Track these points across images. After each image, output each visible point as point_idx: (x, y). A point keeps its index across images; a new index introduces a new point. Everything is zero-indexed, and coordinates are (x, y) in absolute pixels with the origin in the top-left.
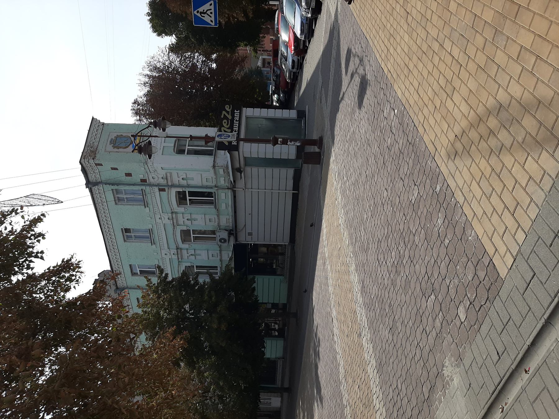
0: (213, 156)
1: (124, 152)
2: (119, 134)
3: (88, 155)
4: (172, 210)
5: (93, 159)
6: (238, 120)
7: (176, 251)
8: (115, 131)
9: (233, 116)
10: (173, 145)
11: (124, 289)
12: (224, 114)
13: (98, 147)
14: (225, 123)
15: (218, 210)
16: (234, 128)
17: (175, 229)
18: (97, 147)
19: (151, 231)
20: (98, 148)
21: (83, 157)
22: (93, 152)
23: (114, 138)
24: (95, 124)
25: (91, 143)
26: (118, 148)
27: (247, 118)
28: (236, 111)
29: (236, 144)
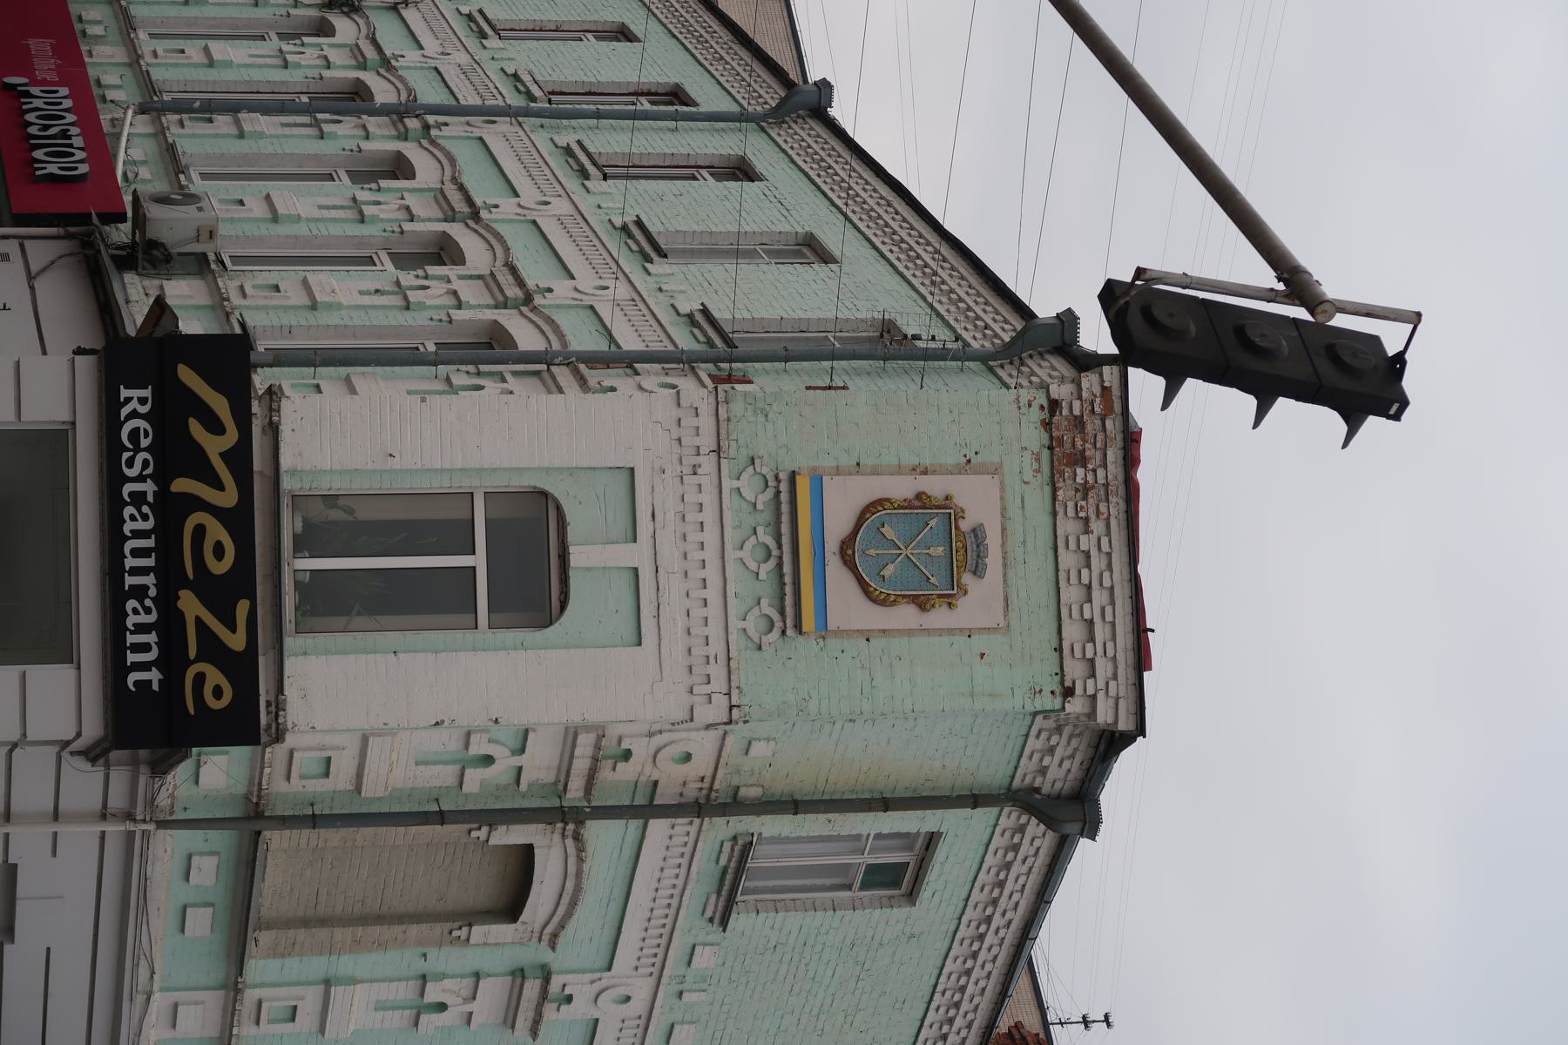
0: (287, 484)
1: (876, 472)
2: (939, 617)
3: (1092, 425)
4: (534, 309)
5: (1054, 405)
6: (132, 604)
7: (484, 214)
8: (979, 643)
9: (170, 624)
10: (579, 557)
11: (778, 115)
14: (219, 551)
15: (228, 315)
17: (499, 263)
18: (1054, 498)
19: (653, 255)
20: (1048, 489)
21: (1117, 407)
23: (967, 579)
24: (1115, 677)
25: (1097, 526)
27: (62, 651)
28: (154, 676)
29: (125, 393)
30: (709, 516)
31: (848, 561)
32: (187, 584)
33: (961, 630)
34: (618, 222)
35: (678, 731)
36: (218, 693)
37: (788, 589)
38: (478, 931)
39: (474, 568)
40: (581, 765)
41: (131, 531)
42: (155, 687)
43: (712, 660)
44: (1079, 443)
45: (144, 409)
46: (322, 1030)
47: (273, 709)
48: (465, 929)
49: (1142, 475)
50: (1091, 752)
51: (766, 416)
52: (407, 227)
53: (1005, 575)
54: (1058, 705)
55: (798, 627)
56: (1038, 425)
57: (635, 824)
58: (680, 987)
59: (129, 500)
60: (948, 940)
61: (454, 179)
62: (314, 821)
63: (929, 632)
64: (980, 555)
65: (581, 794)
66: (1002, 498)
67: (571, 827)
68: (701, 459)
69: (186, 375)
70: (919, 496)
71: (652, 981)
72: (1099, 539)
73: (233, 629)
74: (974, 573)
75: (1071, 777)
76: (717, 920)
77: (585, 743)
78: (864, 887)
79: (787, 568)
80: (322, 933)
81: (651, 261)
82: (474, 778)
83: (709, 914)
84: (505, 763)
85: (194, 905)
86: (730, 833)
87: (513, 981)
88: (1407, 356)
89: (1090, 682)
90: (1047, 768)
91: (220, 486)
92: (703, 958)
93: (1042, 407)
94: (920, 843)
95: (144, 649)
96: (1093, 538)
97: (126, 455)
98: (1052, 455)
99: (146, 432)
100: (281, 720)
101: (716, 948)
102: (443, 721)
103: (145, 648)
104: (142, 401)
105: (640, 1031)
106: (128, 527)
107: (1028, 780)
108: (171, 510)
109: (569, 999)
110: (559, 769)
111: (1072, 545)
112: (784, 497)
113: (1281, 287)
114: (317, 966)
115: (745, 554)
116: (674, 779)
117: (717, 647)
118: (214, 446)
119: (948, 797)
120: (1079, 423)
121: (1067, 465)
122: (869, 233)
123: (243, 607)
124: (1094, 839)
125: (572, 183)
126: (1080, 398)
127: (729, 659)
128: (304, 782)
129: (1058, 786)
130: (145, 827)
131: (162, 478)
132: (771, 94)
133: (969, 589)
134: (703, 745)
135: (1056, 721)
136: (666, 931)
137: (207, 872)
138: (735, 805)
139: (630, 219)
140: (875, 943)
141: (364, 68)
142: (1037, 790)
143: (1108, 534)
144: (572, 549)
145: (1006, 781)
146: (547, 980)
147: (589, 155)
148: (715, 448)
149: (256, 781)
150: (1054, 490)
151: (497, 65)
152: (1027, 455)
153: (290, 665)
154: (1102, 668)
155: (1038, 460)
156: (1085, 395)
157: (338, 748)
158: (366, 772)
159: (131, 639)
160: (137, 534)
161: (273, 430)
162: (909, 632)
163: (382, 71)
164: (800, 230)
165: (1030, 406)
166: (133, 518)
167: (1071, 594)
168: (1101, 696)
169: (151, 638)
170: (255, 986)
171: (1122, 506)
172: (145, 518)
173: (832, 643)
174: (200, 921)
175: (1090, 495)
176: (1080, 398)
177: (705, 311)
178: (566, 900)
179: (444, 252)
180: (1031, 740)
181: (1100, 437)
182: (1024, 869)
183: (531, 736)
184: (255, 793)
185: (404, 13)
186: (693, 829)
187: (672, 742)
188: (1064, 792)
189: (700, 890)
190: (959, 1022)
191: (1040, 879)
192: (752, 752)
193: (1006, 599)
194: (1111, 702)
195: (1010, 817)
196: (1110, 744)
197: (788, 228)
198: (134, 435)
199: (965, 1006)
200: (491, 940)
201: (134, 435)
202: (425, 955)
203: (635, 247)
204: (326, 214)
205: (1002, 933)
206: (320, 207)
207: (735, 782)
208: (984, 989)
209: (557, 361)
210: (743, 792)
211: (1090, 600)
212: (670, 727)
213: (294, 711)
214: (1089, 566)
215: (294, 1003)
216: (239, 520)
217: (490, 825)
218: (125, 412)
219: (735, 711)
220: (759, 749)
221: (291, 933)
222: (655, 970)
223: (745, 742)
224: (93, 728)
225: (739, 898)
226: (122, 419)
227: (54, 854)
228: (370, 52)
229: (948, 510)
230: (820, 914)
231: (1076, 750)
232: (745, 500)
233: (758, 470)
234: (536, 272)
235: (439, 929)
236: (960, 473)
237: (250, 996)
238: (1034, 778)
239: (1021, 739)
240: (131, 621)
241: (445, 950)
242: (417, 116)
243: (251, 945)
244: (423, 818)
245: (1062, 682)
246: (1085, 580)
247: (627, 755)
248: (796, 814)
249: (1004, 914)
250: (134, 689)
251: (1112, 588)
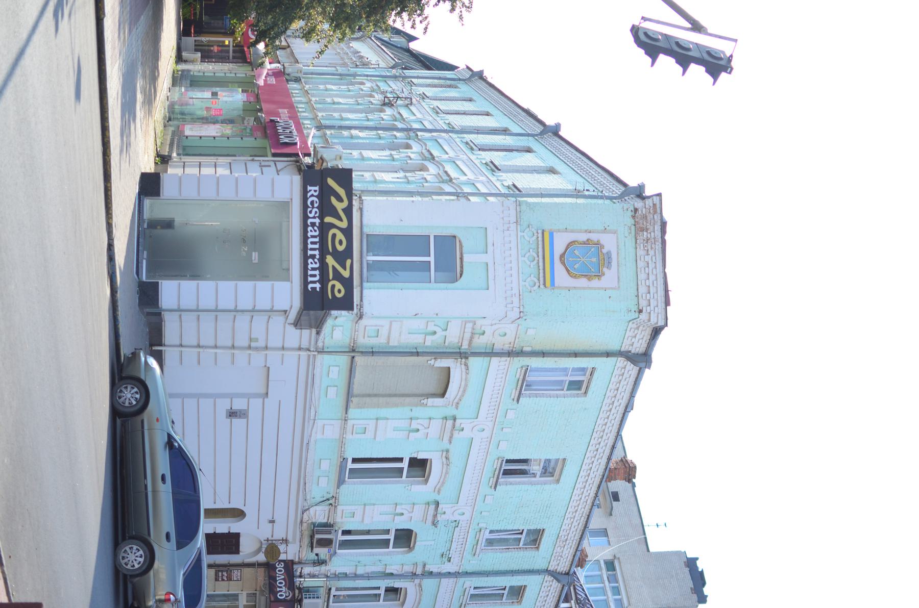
0: (366, 230)
1: (572, 231)
2: (595, 283)
3: (650, 217)
6: (310, 260)
8: (609, 292)
9: (323, 267)
12: (345, 268)
13: (634, 246)
14: (341, 242)
16: (317, 233)
18: (636, 243)
21: (658, 211)
22: (642, 230)
23: (605, 270)
25: (651, 252)
26: (588, 242)
27: (288, 278)
28: (318, 286)
29: (309, 188)
30: (513, 244)
31: (563, 263)
32: (329, 253)
33: (602, 288)
34: (484, 162)
35: (502, 324)
36: (339, 291)
37: (541, 271)
38: (430, 401)
39: (430, 262)
40: (467, 336)
41: (311, 236)
42: (318, 290)
43: (514, 296)
44: (645, 223)
45: (316, 194)
46: (375, 438)
47: (359, 307)
48: (426, 400)
49: (667, 237)
50: (649, 337)
51: (534, 211)
52: (409, 161)
53: (618, 269)
54: (637, 316)
55: (544, 284)
56: (630, 217)
57: (487, 359)
58: (502, 426)
59: (310, 225)
60: (598, 411)
61: (426, 149)
62: (373, 353)
63: (591, 288)
64: (609, 263)
65: (467, 347)
66: (617, 242)
67: (463, 360)
68: (511, 225)
69: (330, 182)
70: (588, 240)
71: (493, 423)
72: (652, 257)
73: (345, 269)
74: (607, 268)
75: (642, 346)
76: (516, 399)
77: (469, 326)
78: (568, 389)
79: (541, 264)
80: (375, 400)
81: (495, 172)
83: (512, 397)
84: (440, 334)
85: (331, 386)
86: (520, 366)
87: (443, 421)
88: (733, 55)
89: (648, 308)
90: (633, 343)
91: (341, 220)
92: (511, 415)
93: (632, 211)
94: (588, 373)
95: (315, 276)
96: (650, 256)
97: (309, 209)
98: (635, 227)
99: (316, 202)
100: (361, 311)
101: (515, 411)
102: (418, 314)
103: (315, 276)
104: (315, 191)
105: (488, 443)
106: (309, 234)
107: (627, 347)
108: (324, 229)
109: (463, 430)
110: (459, 337)
111: (642, 259)
112: (540, 239)
113: (689, 26)
114: (372, 412)
115: (525, 259)
116: (501, 344)
117: (516, 291)
118: (340, 206)
119: (598, 353)
120: (645, 217)
121: (640, 231)
122: (573, 167)
123: (348, 262)
124: (649, 368)
125: (468, 152)
126: (645, 207)
127: (520, 295)
128: (369, 339)
129: (638, 350)
130: (314, 353)
131: (321, 218)
132: (538, 129)
133: (606, 273)
134: (511, 330)
135: (637, 324)
136: (497, 404)
137: (335, 370)
138: (521, 353)
139: (488, 161)
141: (396, 121)
142: (630, 352)
143: (655, 255)
144: (464, 255)
145: (618, 348)
146: (455, 419)
147: (474, 144)
148: (515, 221)
149: (353, 337)
150: (636, 240)
151: (443, 121)
152: (626, 227)
153: (365, 292)
154: (653, 303)
155: (630, 229)
156: (647, 207)
157: (382, 326)
159: (310, 273)
160: (313, 237)
161: (361, 209)
162: (584, 288)
163: (402, 121)
164: (548, 165)
165: (627, 210)
166: (311, 231)
167: (642, 276)
168: (652, 312)
169: (317, 272)
170: (351, 419)
171: (660, 246)
172: (315, 231)
173: (556, 291)
174: (332, 392)
175: (649, 241)
176: (645, 207)
177: (514, 185)
178: (462, 389)
179: (423, 168)
180: (628, 332)
181: (652, 221)
182: (626, 383)
183: (449, 323)
184: (352, 342)
185: (412, 108)
186: (507, 363)
187: (500, 328)
188: (639, 353)
189: (511, 390)
190: (602, 444)
191: (631, 387)
192: (528, 333)
193: (619, 278)
194: (656, 315)
195: (621, 361)
196: (656, 332)
197: (544, 165)
198: (312, 203)
199: (604, 437)
200: (435, 405)
201: (312, 203)
202: (411, 410)
203: (489, 168)
204: (381, 158)
205: (617, 408)
206: (379, 156)
207: (522, 345)
208: (611, 431)
209: (460, 195)
211: (648, 279)
212: (498, 322)
213: (366, 309)
214: (648, 267)
215: (365, 426)
216: (348, 232)
217: (435, 358)
218: (309, 194)
219: (521, 313)
220: (530, 332)
221: (364, 399)
222: (493, 419)
223: (526, 329)
224: (297, 303)
225: (523, 392)
226: (308, 197)
227: (282, 364)
228: (398, 116)
229: (598, 244)
230: (552, 398)
231: (644, 336)
232: (526, 239)
233: (531, 229)
234: (453, 174)
235: (416, 399)
236: (602, 233)
237: (350, 423)
239: (624, 332)
240: (310, 266)
241: (419, 408)
242: (414, 132)
243: (351, 405)
244: (411, 354)
245: (638, 308)
246: (647, 272)
247: (484, 333)
248: (543, 357)
249: (618, 401)
250: (310, 290)
251: (657, 274)
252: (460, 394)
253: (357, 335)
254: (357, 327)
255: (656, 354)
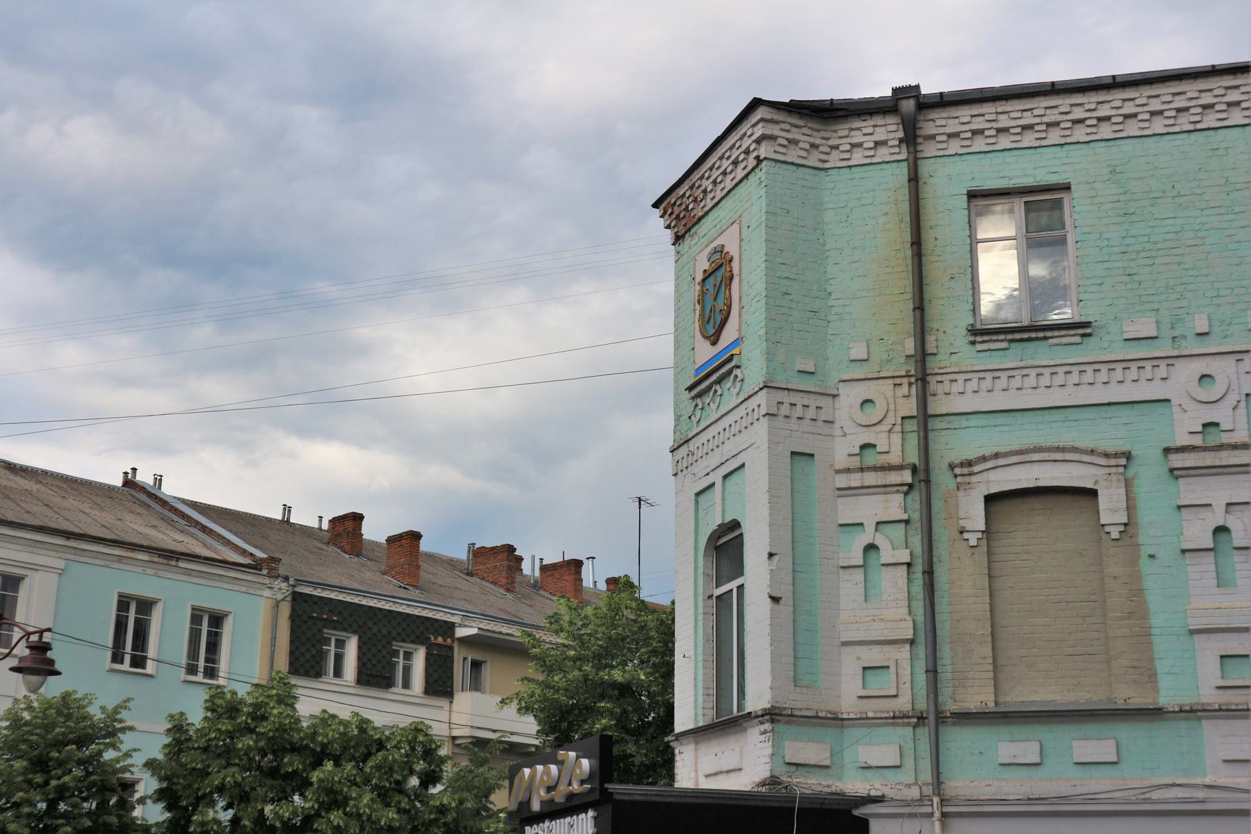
40: (871, 478)
82: (887, 554)
124: (918, 87)
129: (894, 128)
140: (1122, 198)
149: (891, 721)
158: (883, 638)
178: (1059, 456)
202: (1152, 556)
210: (911, 351)
238: (892, 147)
252: (1076, 457)
253: (875, 712)
254: (852, 716)
255: (882, 90)
